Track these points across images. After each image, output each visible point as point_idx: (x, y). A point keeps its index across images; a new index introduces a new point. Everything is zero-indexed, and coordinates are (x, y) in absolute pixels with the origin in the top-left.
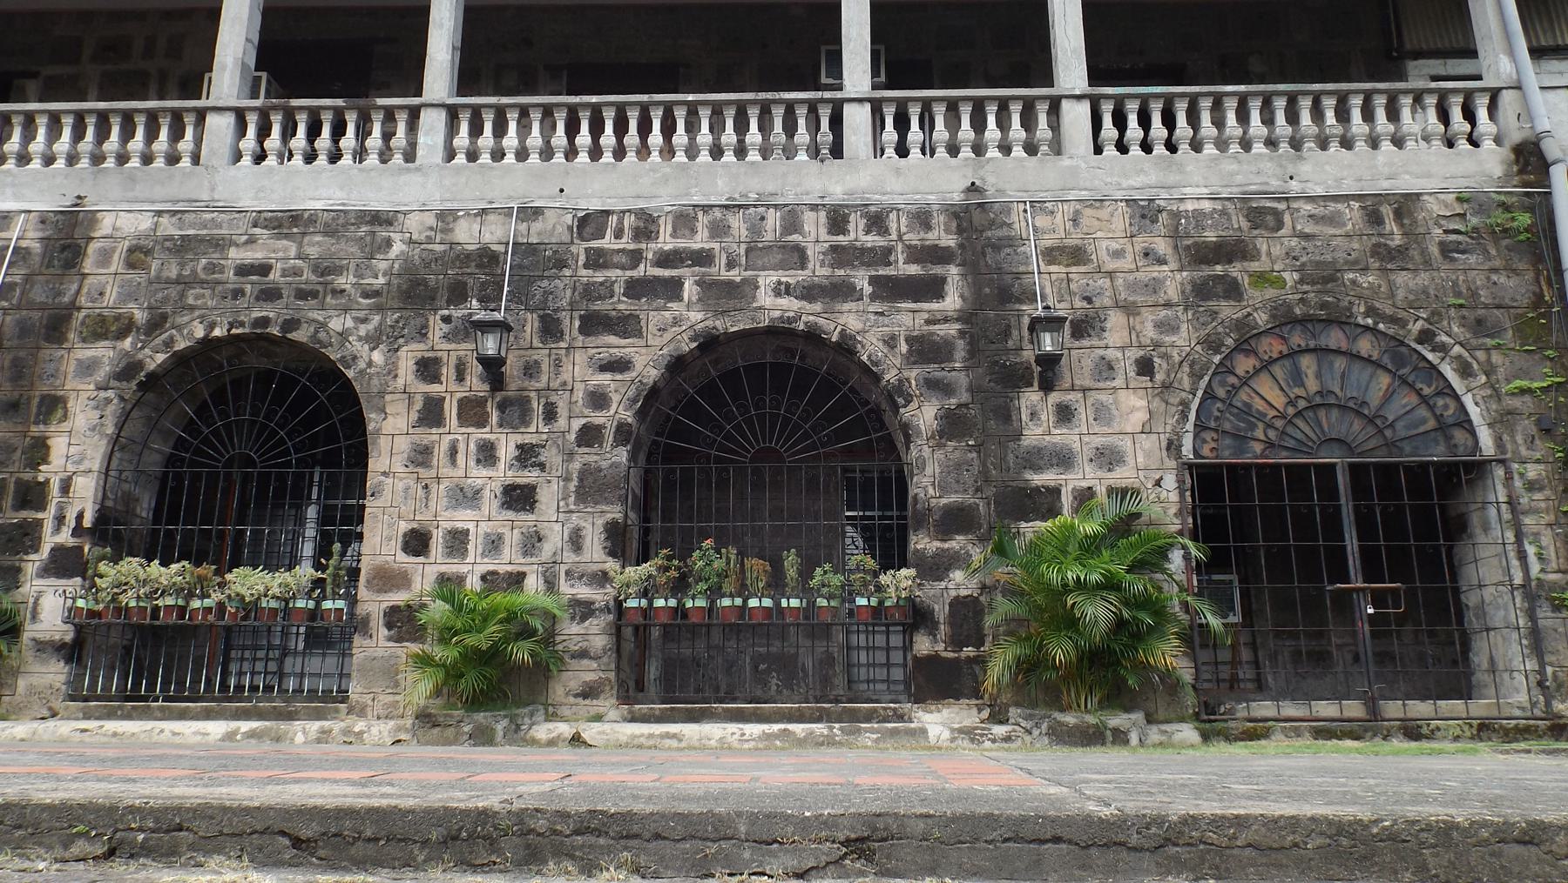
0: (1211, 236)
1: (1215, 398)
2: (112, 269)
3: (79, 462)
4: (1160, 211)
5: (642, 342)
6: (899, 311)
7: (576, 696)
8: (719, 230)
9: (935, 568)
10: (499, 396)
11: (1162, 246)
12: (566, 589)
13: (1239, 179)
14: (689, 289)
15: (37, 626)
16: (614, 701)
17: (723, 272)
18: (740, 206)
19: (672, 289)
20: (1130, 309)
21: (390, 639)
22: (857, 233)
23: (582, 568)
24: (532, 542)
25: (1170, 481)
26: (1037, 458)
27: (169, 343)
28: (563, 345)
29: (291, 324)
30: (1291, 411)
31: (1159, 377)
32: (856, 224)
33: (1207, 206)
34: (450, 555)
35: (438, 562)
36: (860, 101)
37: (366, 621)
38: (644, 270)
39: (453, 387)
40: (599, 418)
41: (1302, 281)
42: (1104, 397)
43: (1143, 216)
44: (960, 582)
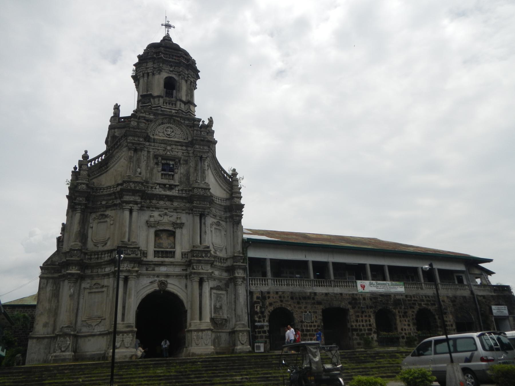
11: (449, 300)
14: (417, 304)
20: (449, 307)
22: (428, 299)
24: (411, 329)
35: (404, 332)
38: (413, 302)
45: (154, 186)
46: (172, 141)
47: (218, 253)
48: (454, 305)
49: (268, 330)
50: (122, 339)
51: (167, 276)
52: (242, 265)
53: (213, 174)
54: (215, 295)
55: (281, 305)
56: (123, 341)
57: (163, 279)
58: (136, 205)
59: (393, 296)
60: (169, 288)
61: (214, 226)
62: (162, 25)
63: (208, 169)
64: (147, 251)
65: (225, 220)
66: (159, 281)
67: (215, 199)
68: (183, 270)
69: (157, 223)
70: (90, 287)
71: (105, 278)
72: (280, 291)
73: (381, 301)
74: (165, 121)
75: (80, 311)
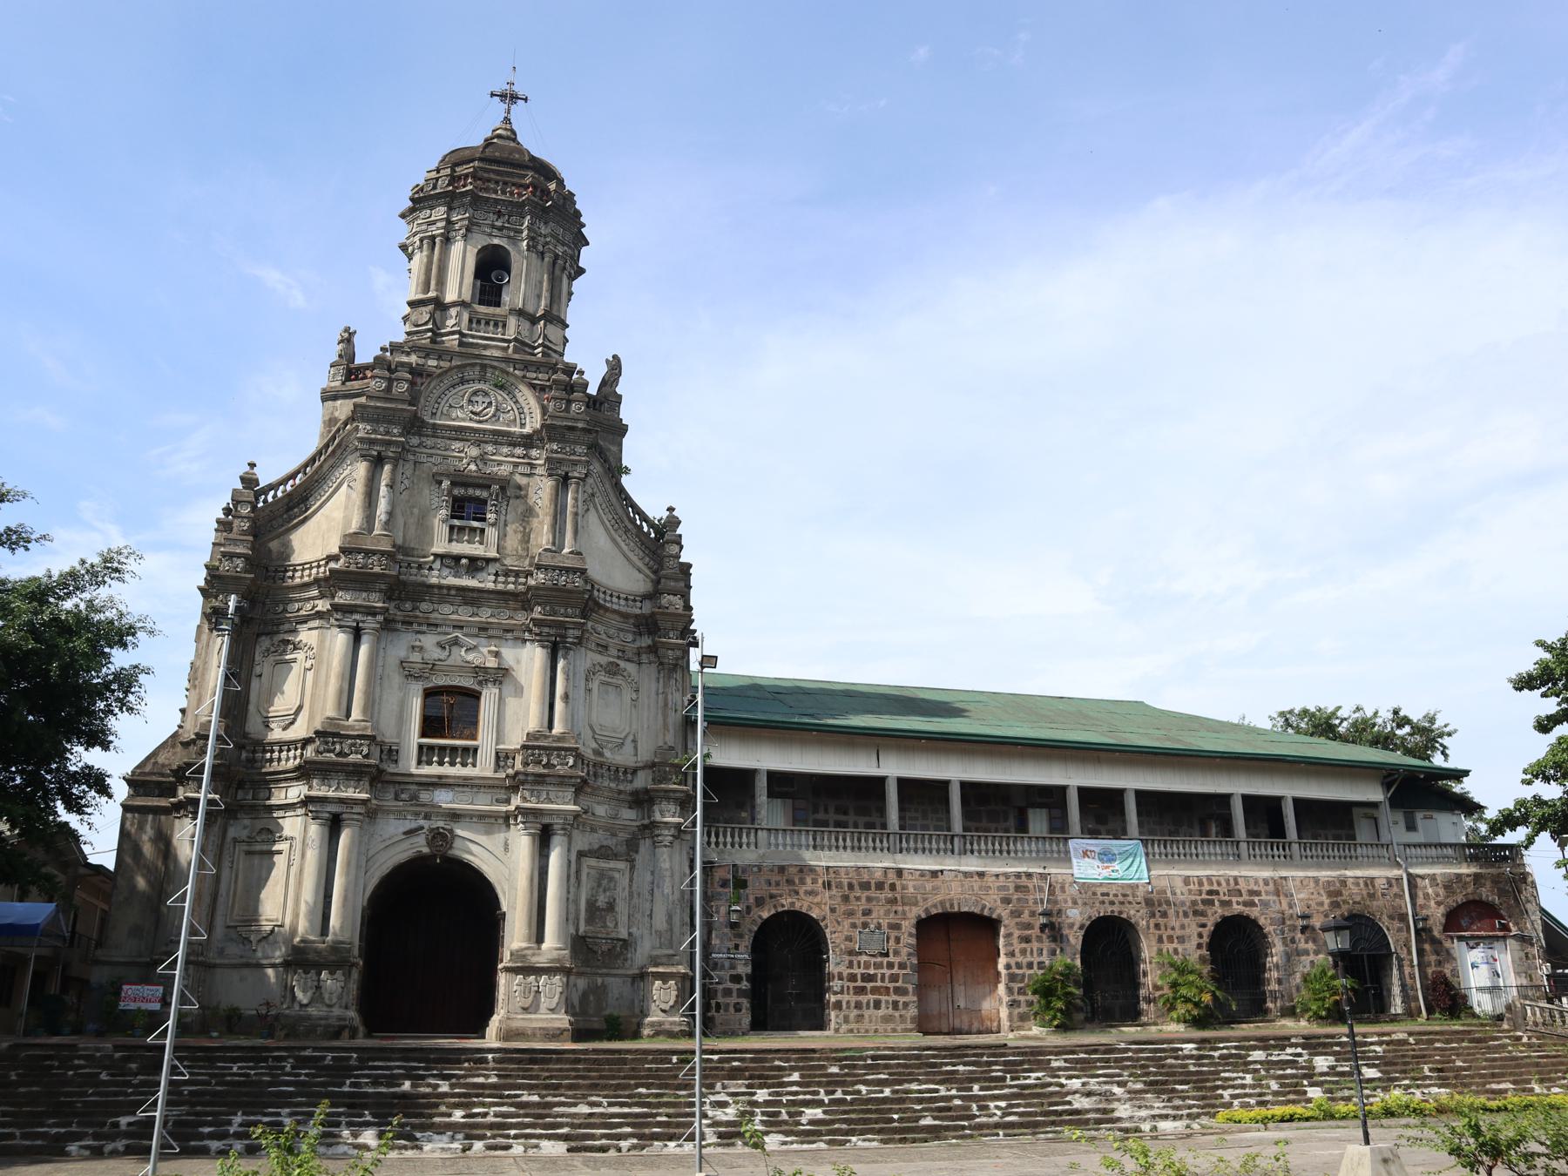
0: (1332, 888)
8: (1219, 884)
11: (1322, 892)
14: (1217, 903)
19: (1211, 903)
38: (1204, 896)
40: (1201, 941)
41: (1354, 903)
45: (426, 563)
46: (485, 431)
47: (607, 754)
48: (1335, 905)
49: (747, 975)
50: (316, 983)
51: (455, 816)
52: (675, 791)
53: (603, 523)
54: (593, 872)
55: (793, 904)
56: (318, 987)
57: (441, 824)
58: (369, 618)
60: (459, 849)
61: (602, 677)
62: (493, 95)
63: (588, 509)
64: (397, 744)
65: (636, 659)
66: (431, 830)
67: (608, 598)
68: (497, 801)
69: (430, 666)
70: (249, 837)
71: (287, 814)
72: (791, 866)
73: (1108, 895)
74: (469, 373)
75: (221, 900)
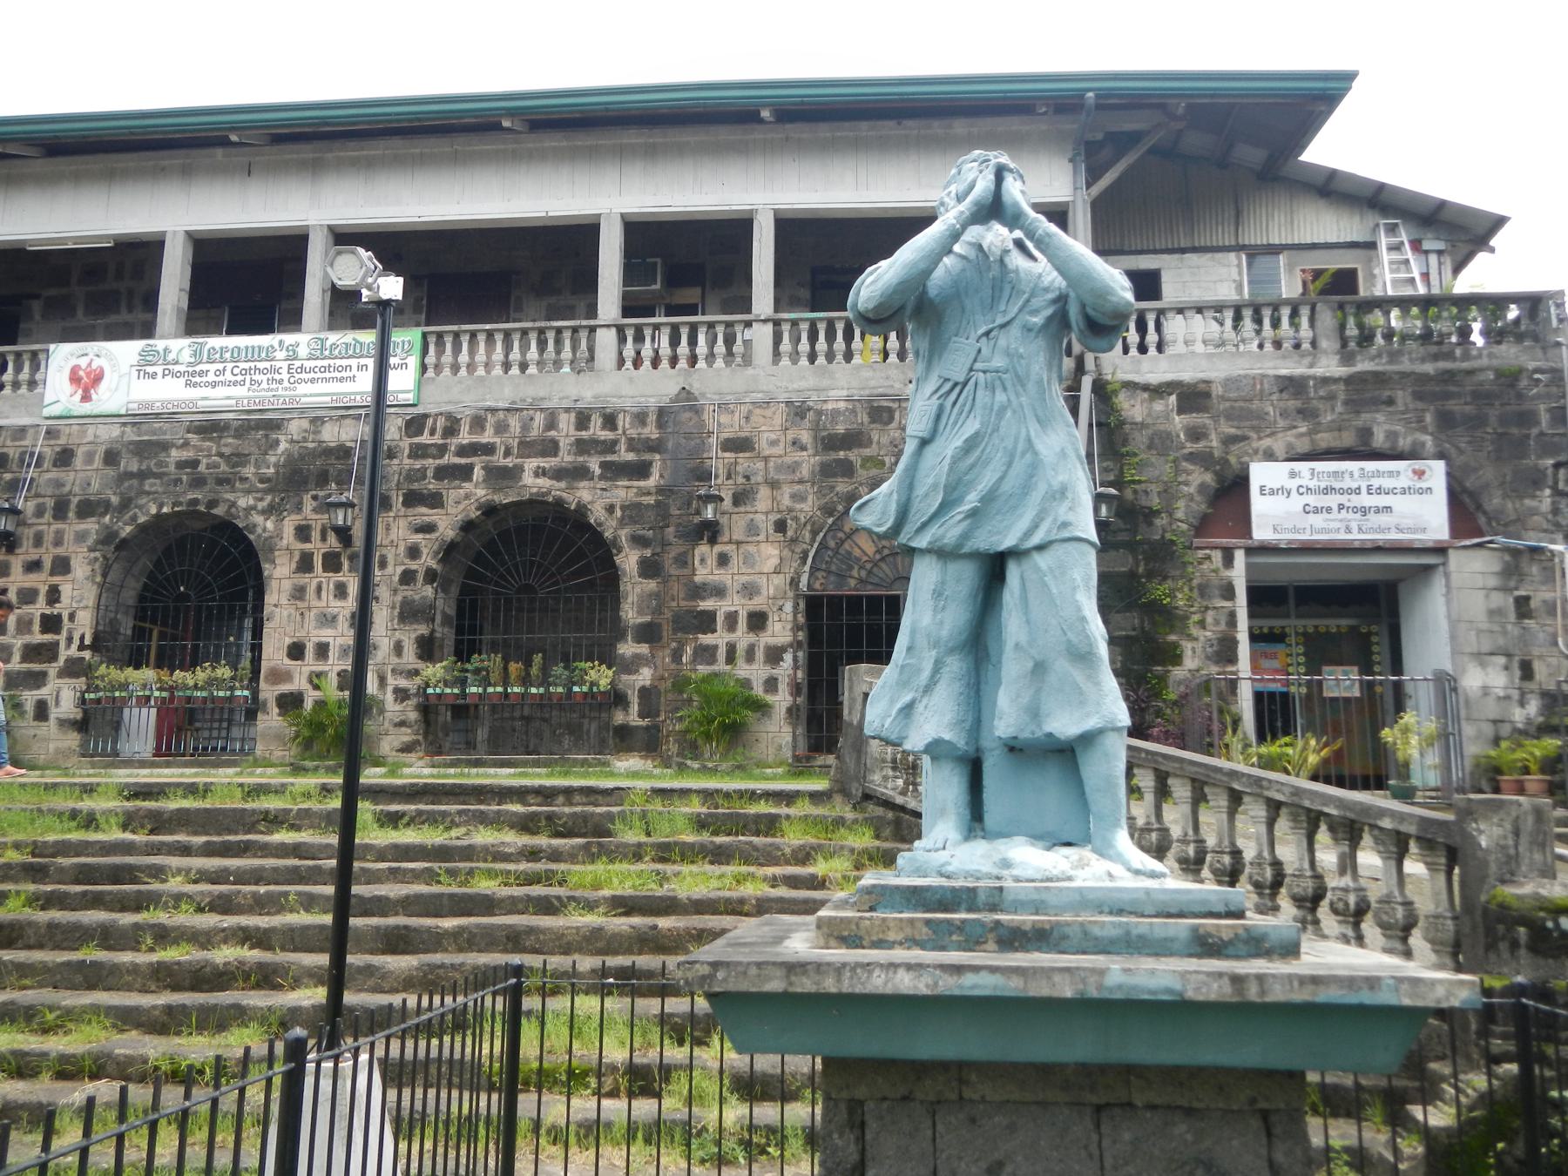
0: (840, 429)
1: (827, 548)
2: (95, 466)
3: (80, 601)
4: (809, 410)
5: (443, 511)
6: (617, 487)
7: (398, 751)
8: (501, 428)
9: (631, 666)
10: (349, 551)
11: (806, 437)
12: (392, 681)
13: (873, 383)
14: (478, 473)
15: (58, 710)
16: (421, 754)
17: (501, 460)
18: (517, 410)
20: (774, 485)
21: (279, 715)
22: (596, 430)
23: (402, 667)
25: (789, 607)
26: (698, 591)
27: (134, 518)
28: (392, 514)
29: (212, 504)
30: (878, 557)
31: (790, 533)
32: (596, 422)
33: (842, 405)
34: (317, 659)
35: (310, 664)
36: (608, 326)
37: (265, 703)
38: (450, 459)
39: (319, 545)
40: (413, 565)
42: (751, 548)
43: (796, 414)
44: (645, 676)
59: (296, 427)
